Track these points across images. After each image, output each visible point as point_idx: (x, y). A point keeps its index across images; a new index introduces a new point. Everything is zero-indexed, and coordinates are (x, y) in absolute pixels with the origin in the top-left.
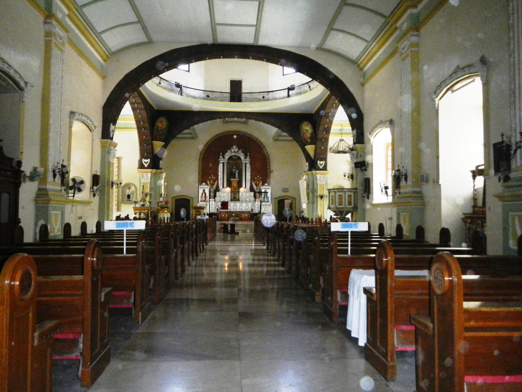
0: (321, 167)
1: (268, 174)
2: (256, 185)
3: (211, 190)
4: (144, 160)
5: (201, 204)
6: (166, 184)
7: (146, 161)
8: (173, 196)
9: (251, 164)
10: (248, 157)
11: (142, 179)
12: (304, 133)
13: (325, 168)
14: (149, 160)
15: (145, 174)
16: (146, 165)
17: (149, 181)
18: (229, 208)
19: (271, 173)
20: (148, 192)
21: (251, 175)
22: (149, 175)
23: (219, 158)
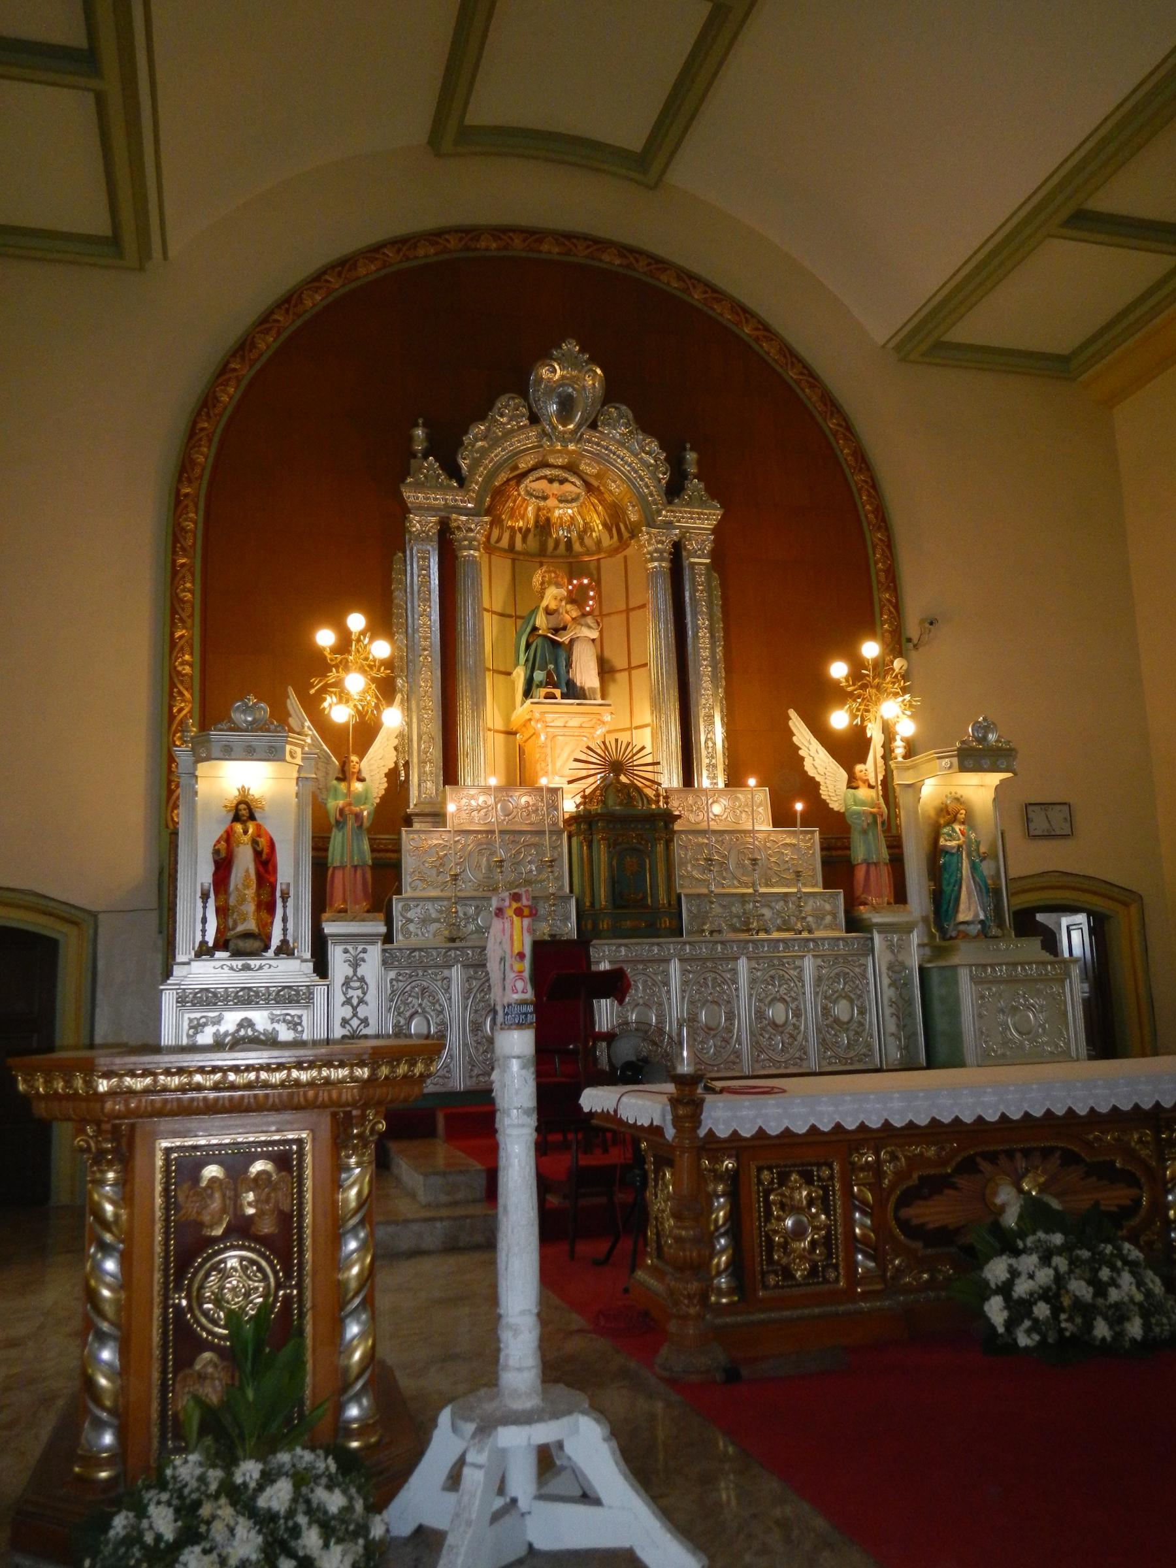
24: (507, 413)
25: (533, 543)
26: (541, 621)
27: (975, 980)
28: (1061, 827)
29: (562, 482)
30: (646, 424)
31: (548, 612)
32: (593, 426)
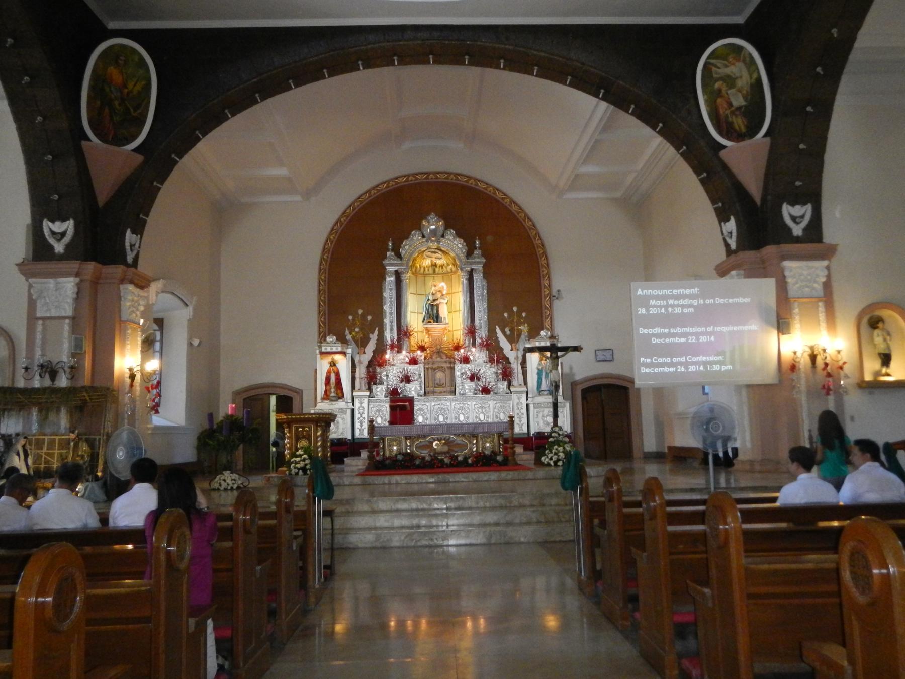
0: (797, 231)
1: (546, 303)
2: (513, 339)
3: (357, 360)
4: (47, 225)
5: (323, 407)
6: (196, 342)
7: (58, 227)
8: (238, 386)
9: (486, 275)
10: (477, 252)
11: (39, 305)
12: (720, 90)
13: (814, 232)
14: (68, 226)
15: (51, 280)
16: (59, 248)
17: (68, 311)
18: (420, 419)
19: (557, 304)
20: (65, 359)
21: (490, 309)
22: (69, 284)
23: (385, 257)
24: (416, 236)
25: (431, 271)
26: (431, 298)
27: (535, 408)
28: (609, 357)
29: (435, 253)
30: (459, 235)
31: (433, 294)
32: (443, 236)
